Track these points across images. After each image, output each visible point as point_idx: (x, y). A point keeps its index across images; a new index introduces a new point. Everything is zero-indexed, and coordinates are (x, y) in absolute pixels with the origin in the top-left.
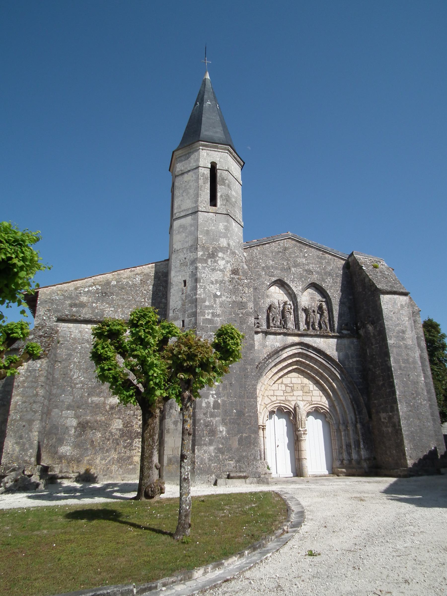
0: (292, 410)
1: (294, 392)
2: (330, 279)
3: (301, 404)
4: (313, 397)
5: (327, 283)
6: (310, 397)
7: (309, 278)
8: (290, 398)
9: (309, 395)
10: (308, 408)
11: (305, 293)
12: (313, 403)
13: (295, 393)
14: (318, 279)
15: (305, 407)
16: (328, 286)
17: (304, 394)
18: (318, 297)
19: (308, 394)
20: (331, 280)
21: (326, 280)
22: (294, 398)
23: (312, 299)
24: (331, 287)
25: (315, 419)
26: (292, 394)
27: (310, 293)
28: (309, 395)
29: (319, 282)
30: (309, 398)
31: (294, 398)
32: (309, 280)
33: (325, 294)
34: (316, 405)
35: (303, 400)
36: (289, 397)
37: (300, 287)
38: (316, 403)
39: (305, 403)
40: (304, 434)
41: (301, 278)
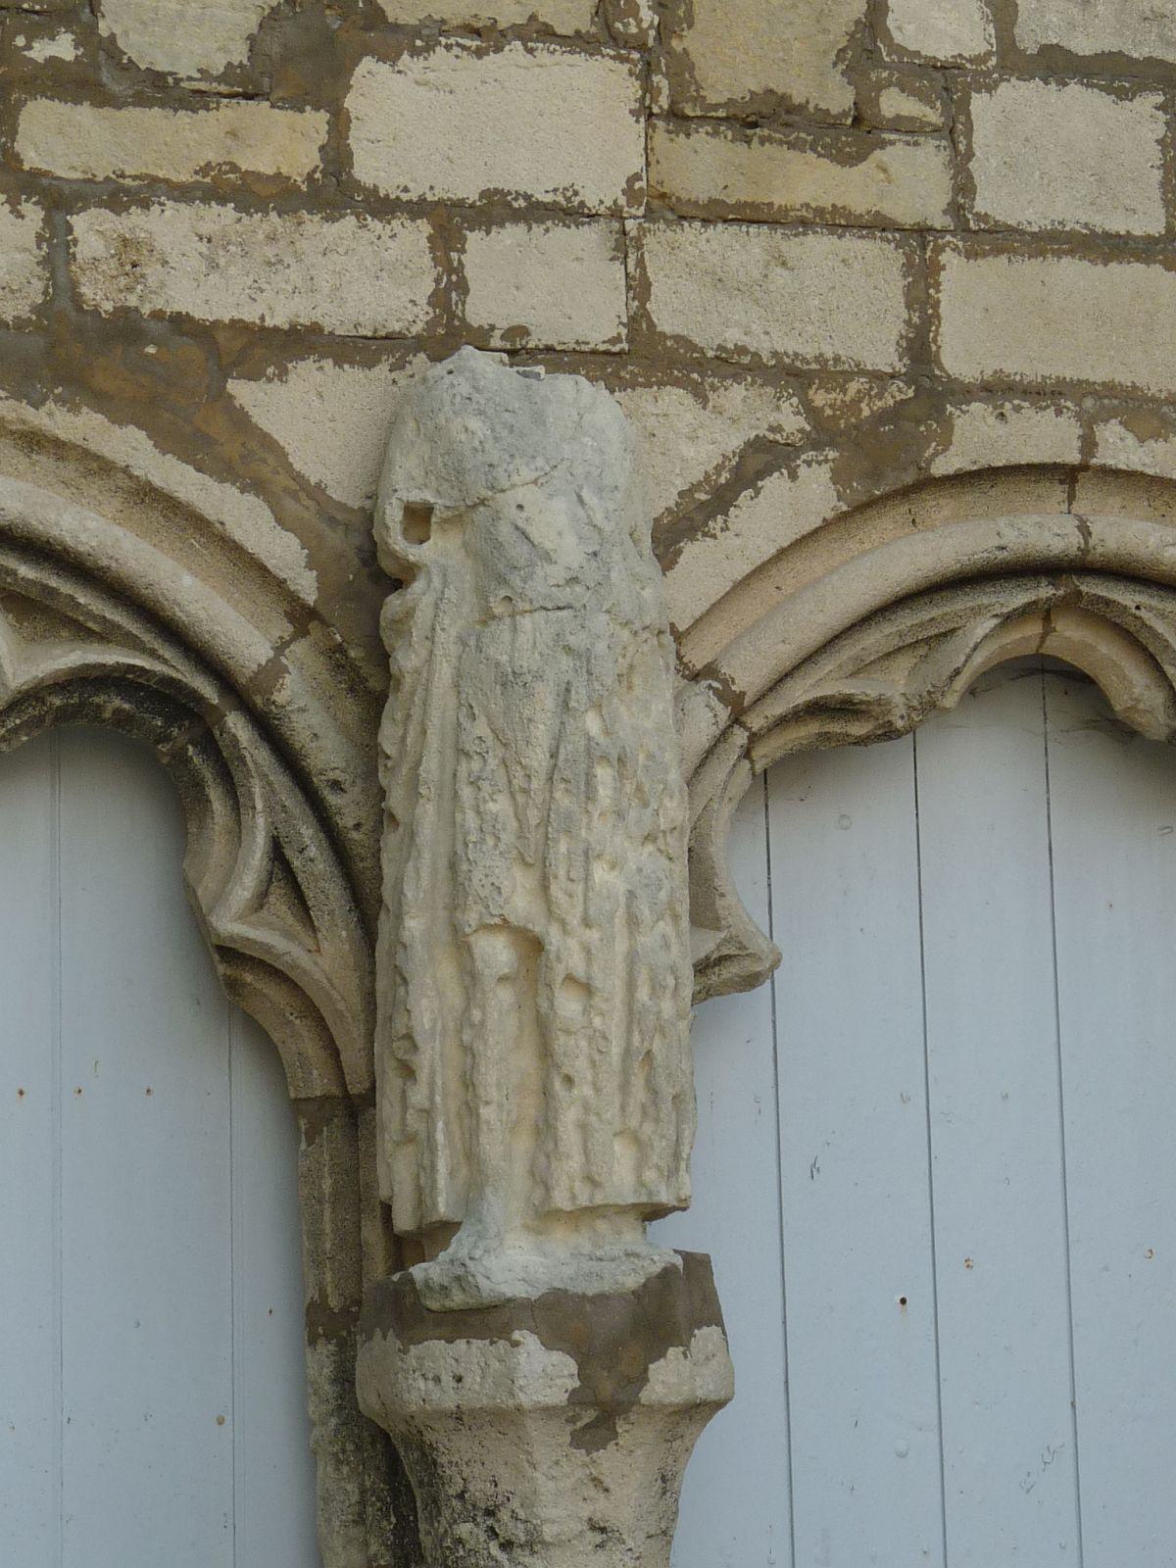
0: (245, 635)
1: (379, 91)
3: (583, 467)
4: (955, 269)
6: (878, 266)
8: (196, 270)
9: (851, 187)
10: (810, 572)
12: (977, 436)
13: (410, 120)
15: (709, 565)
17: (704, 164)
19: (807, 179)
22: (370, 277)
25: (708, 1256)
26: (282, 141)
28: (851, 187)
30: (839, 306)
31: (370, 277)
34: (1042, 527)
35: (642, 357)
36: (169, 227)
38: (1048, 436)
39: (699, 435)
40: (598, 1416)
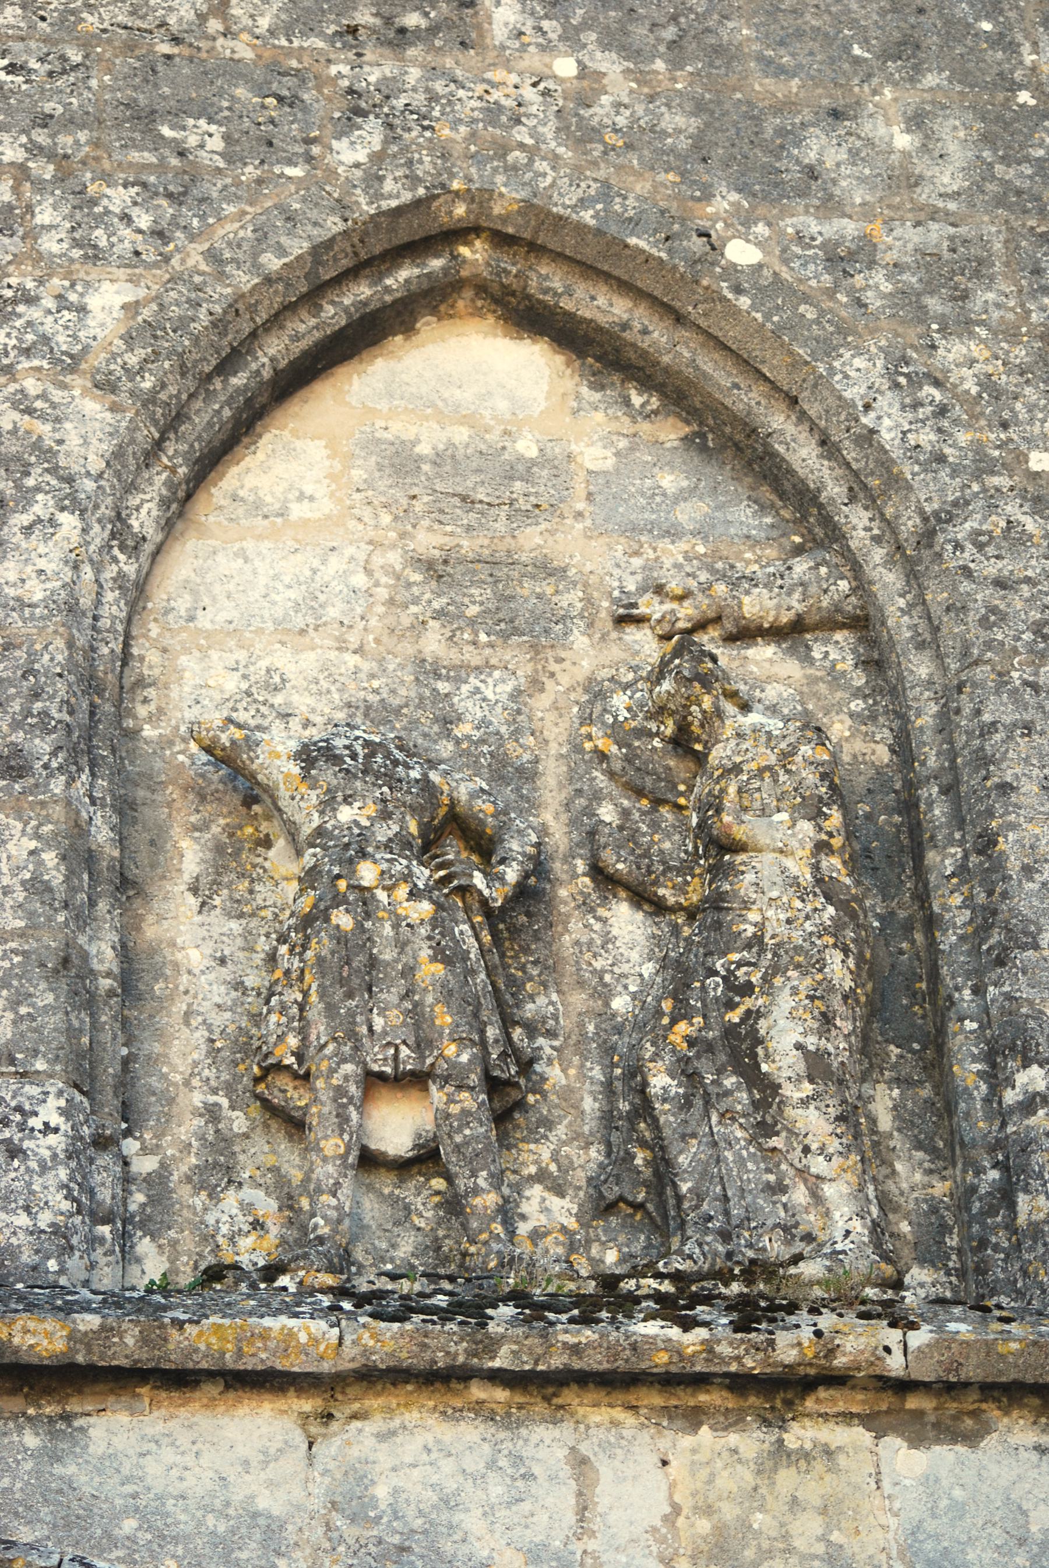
2: (916, 121)
5: (831, 206)
7: (356, 108)
11: (297, 462)
14: (582, 135)
16: (841, 260)
18: (612, 497)
20: (955, 136)
21: (819, 147)
23: (492, 594)
24: (953, 274)
27: (401, 462)
29: (642, 188)
32: (350, 153)
33: (803, 456)
37: (108, 300)
41: (144, 119)
